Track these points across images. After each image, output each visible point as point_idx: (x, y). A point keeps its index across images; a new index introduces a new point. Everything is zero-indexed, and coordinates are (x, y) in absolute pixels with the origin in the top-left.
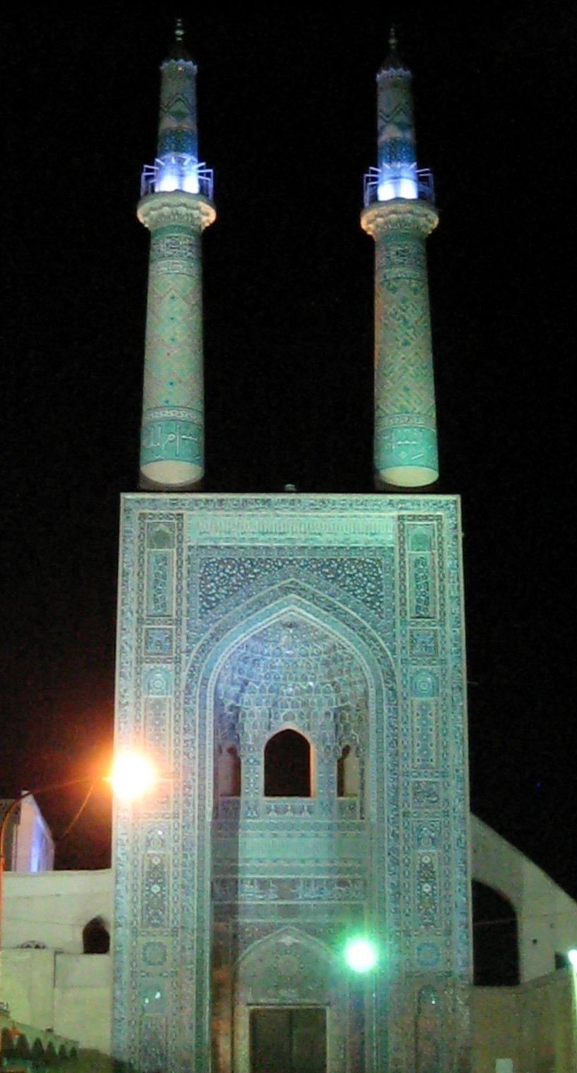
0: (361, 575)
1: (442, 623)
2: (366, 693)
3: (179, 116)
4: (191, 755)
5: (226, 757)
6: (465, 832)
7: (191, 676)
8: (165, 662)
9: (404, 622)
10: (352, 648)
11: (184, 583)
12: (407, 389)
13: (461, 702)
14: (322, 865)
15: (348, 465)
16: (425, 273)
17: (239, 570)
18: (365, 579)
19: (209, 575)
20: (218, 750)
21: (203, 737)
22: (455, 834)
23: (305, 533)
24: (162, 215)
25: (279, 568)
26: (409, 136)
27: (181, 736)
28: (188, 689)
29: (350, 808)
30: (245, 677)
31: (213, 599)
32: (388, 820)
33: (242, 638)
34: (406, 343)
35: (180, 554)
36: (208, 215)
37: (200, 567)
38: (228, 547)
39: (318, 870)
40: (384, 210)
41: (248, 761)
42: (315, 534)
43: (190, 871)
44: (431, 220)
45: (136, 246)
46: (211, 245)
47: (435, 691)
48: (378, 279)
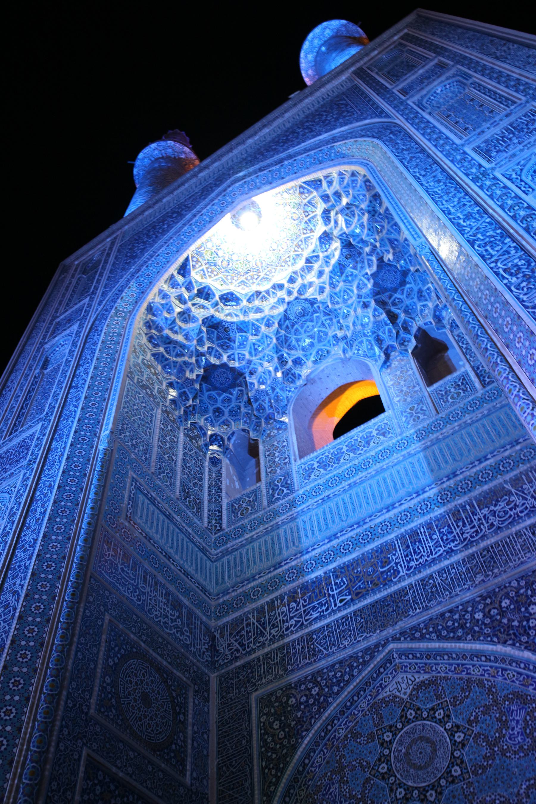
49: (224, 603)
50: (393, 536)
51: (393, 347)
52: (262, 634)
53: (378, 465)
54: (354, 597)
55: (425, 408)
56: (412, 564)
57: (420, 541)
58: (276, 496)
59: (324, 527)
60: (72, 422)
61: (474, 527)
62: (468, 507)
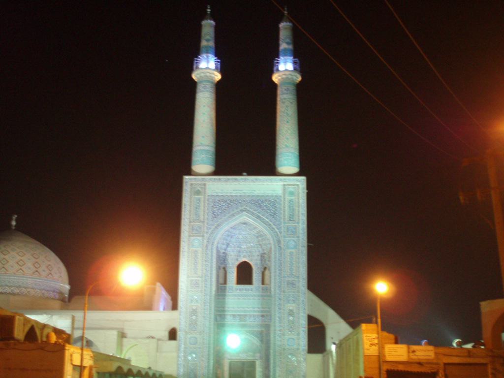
1: (298, 223)
2: (271, 249)
3: (208, 40)
5: (222, 271)
6: (305, 298)
8: (199, 236)
9: (285, 223)
10: (266, 232)
11: (206, 208)
12: (287, 139)
13: (304, 251)
14: (256, 309)
15: (266, 166)
16: (295, 96)
20: (218, 268)
21: (212, 263)
22: (301, 299)
24: (201, 77)
26: (291, 47)
27: (204, 263)
28: (207, 246)
30: (228, 242)
33: (227, 228)
34: (287, 122)
35: (204, 198)
36: (218, 77)
38: (222, 196)
39: (254, 311)
40: (281, 74)
44: (298, 78)
45: (191, 87)
46: (219, 87)
47: (295, 247)
48: (278, 99)
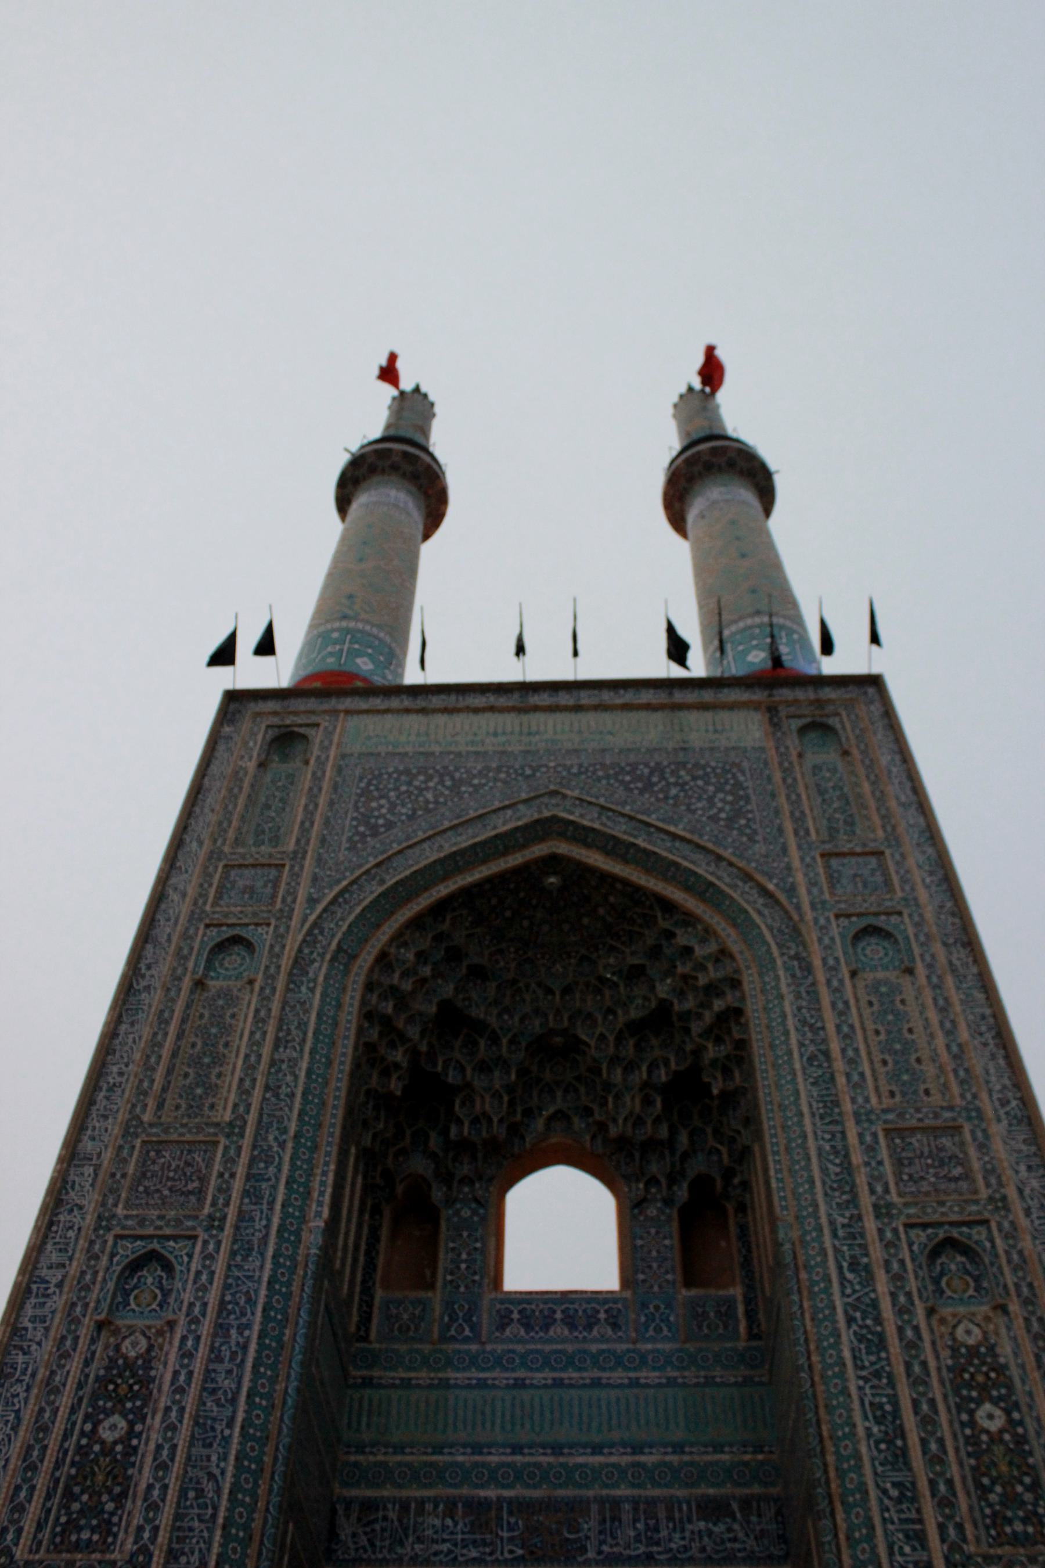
0: (700, 783)
4: (284, 1090)
7: (309, 940)
17: (442, 782)
18: (711, 788)
19: (377, 789)
23: (580, 732)
25: (528, 777)
29: (718, 1313)
31: (381, 821)
32: (835, 1235)
37: (361, 779)
41: (457, 1213)
42: (601, 733)
43: (229, 1372)
49: (356, 1464)
50: (591, 1493)
51: (658, 1182)
52: (402, 1544)
53: (596, 1373)
54: (527, 1557)
55: (672, 1319)
56: (605, 1548)
57: (620, 1521)
58: (453, 1332)
59: (509, 1427)
60: (277, 1179)
61: (683, 1538)
62: (685, 1507)
